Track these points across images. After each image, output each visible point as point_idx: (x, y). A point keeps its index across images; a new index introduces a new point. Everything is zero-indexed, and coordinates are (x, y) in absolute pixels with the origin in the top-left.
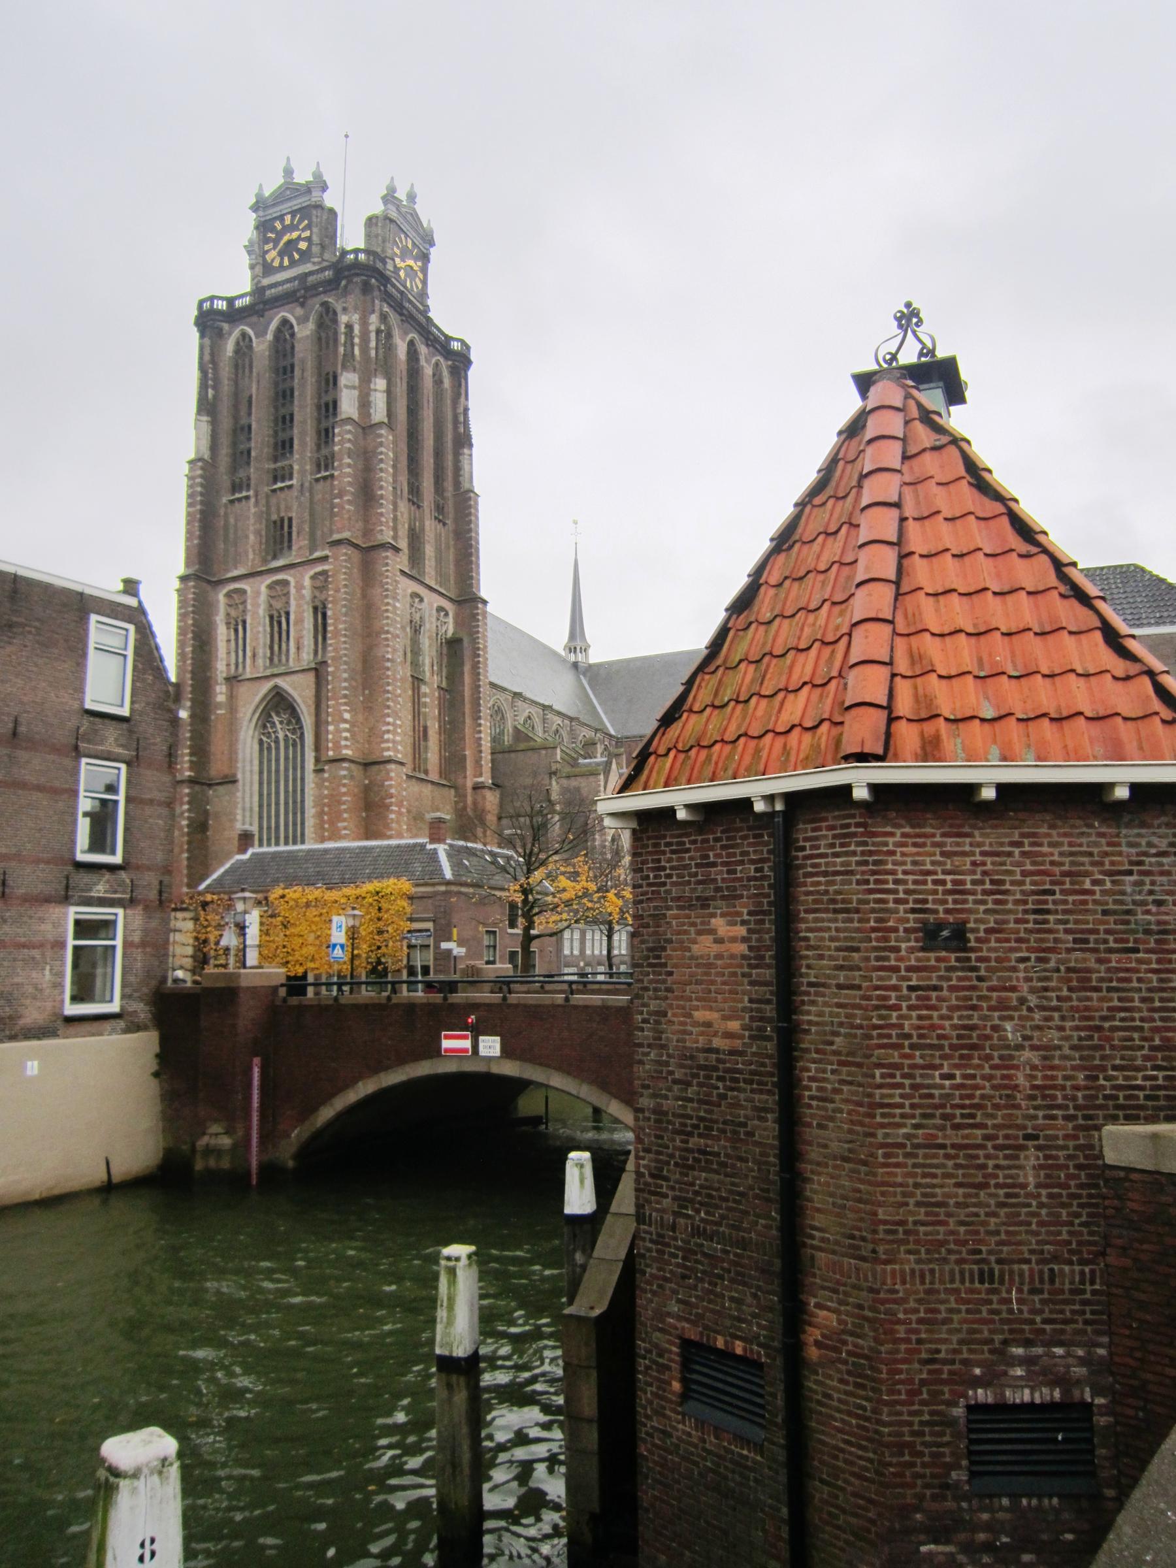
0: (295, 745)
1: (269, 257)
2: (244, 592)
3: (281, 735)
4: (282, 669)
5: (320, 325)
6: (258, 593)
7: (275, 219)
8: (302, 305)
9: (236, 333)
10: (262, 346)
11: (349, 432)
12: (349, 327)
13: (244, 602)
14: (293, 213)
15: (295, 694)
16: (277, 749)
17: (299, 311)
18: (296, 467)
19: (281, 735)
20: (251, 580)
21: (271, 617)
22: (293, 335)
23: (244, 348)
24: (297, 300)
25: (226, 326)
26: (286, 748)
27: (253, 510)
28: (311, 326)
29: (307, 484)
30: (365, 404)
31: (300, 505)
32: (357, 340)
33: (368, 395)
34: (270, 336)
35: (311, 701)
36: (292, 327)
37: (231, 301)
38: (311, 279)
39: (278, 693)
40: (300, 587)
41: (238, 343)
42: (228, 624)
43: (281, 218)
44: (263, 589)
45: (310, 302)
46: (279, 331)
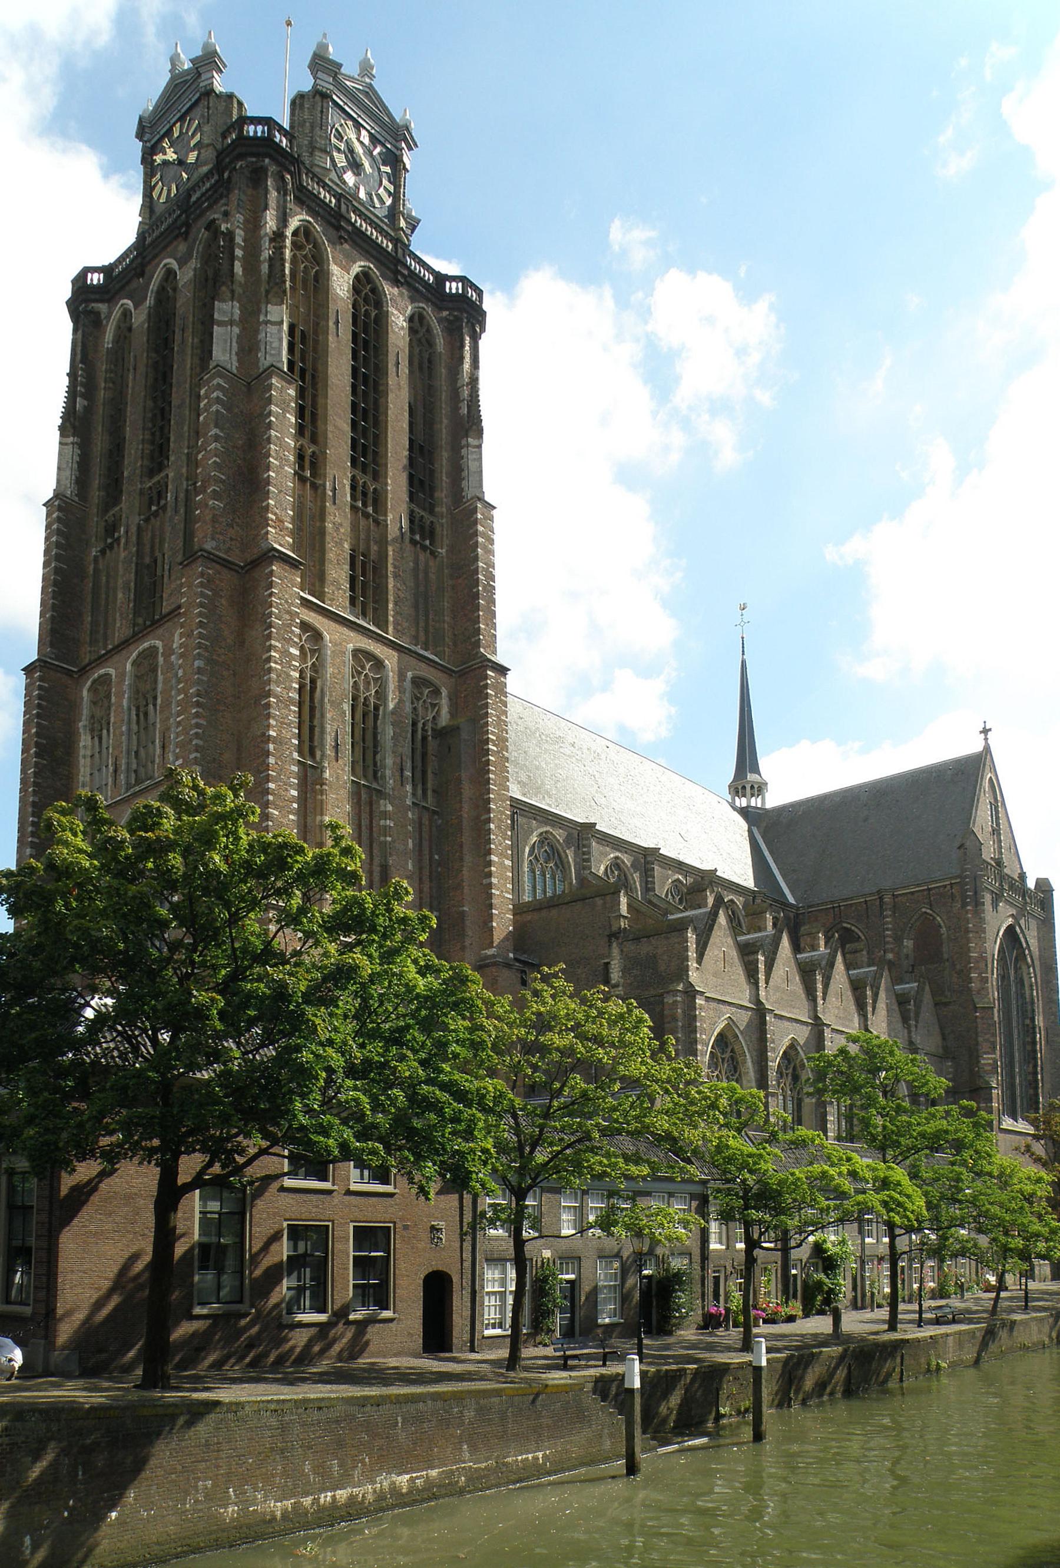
1: (155, 195)
5: (209, 258)
9: (117, 313)
10: (140, 318)
11: (219, 387)
12: (230, 236)
13: (108, 696)
17: (182, 247)
18: (171, 475)
22: (175, 289)
23: (125, 329)
25: (102, 307)
27: (123, 555)
28: (194, 263)
29: (182, 495)
30: (249, 345)
32: (239, 253)
33: (257, 332)
37: (106, 270)
38: (194, 199)
41: (118, 327)
46: (161, 290)
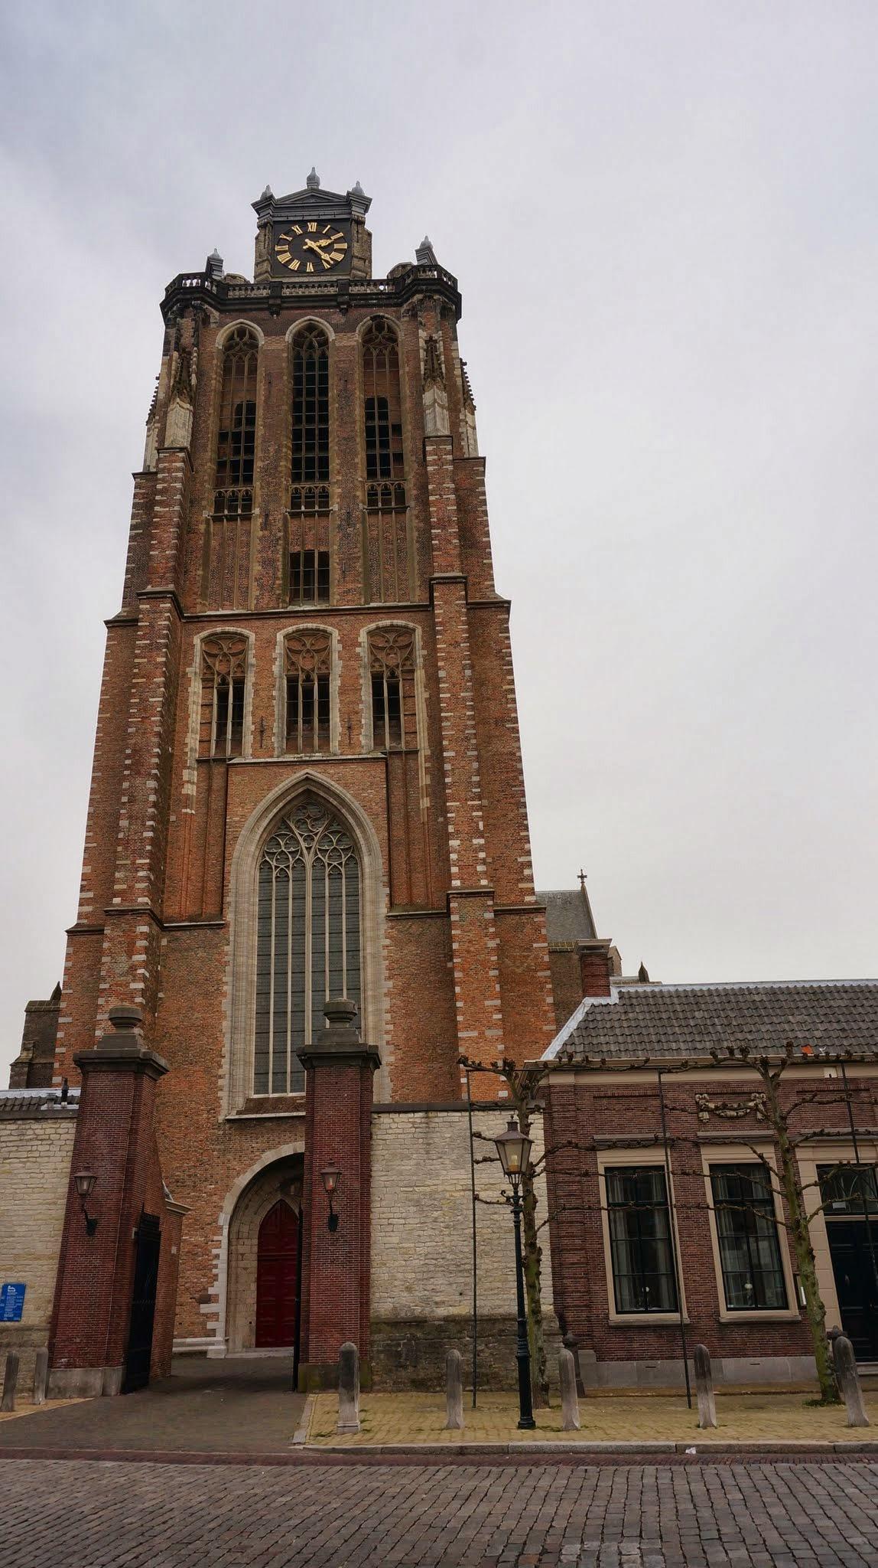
0: (335, 876)
2: (243, 639)
3: (309, 859)
4: (318, 756)
6: (271, 643)
7: (295, 222)
8: (345, 312)
9: (231, 326)
10: (274, 346)
14: (321, 223)
15: (348, 796)
16: (300, 880)
17: (339, 318)
19: (309, 859)
20: (258, 623)
21: (292, 682)
24: (338, 306)
26: (318, 880)
31: (346, 536)
34: (288, 337)
35: (379, 808)
36: (322, 333)
39: (308, 792)
40: (349, 643)
41: (231, 338)
42: (207, 682)
43: (303, 224)
44: (280, 637)
45: (355, 313)
